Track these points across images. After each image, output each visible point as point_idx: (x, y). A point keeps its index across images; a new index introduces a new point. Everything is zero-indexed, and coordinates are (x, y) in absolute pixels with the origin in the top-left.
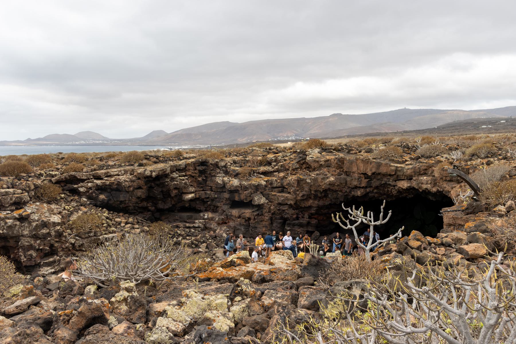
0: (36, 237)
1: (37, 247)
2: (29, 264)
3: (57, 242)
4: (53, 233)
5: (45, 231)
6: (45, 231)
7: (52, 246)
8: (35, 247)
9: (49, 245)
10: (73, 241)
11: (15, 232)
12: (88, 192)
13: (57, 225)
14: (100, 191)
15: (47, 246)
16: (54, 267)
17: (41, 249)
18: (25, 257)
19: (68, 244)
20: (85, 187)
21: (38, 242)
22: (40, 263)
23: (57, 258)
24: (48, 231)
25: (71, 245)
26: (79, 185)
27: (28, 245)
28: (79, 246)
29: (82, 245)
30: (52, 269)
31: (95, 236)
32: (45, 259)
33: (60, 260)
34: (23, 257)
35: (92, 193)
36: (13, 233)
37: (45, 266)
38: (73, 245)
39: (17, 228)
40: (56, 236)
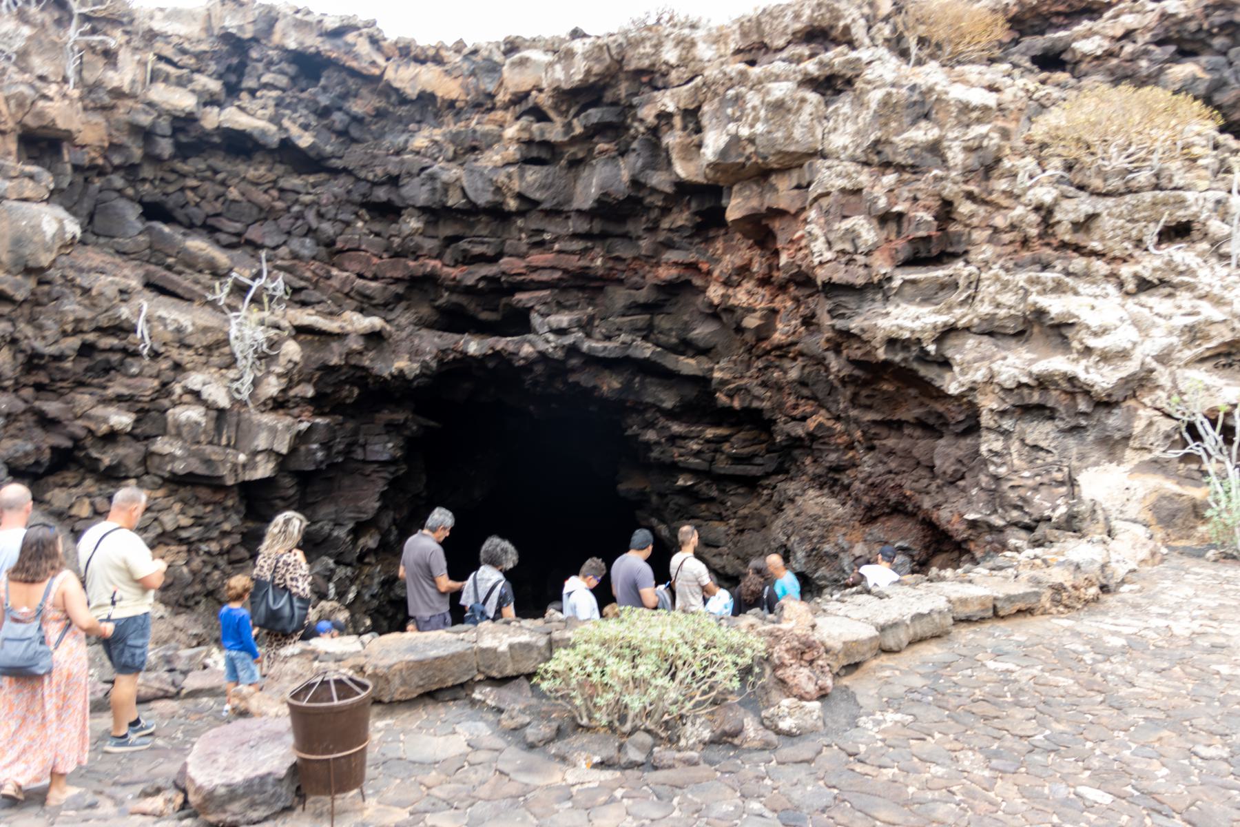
0: (877, 157)
1: (882, 203)
2: (840, 275)
3: (970, 196)
4: (956, 155)
5: (923, 133)
6: (923, 133)
7: (946, 212)
8: (874, 201)
9: (936, 204)
10: (1046, 195)
11: (798, 133)
12: (1110, 54)
13: (979, 121)
14: (1172, 48)
15: (927, 208)
16: (950, 308)
17: (900, 216)
18: (829, 244)
19: (1020, 210)
20: (1105, 37)
21: (890, 178)
22: (890, 279)
23: (959, 269)
24: (934, 133)
25: (1034, 218)
26: (1077, 28)
27: (843, 191)
28: (1077, 226)
29: (1092, 217)
30: (938, 312)
31: (1156, 187)
32: (912, 269)
33: (979, 280)
34: (819, 245)
35: (1133, 58)
36: (789, 137)
37: (910, 301)
38: (1045, 212)
39: (805, 117)
40: (968, 173)
